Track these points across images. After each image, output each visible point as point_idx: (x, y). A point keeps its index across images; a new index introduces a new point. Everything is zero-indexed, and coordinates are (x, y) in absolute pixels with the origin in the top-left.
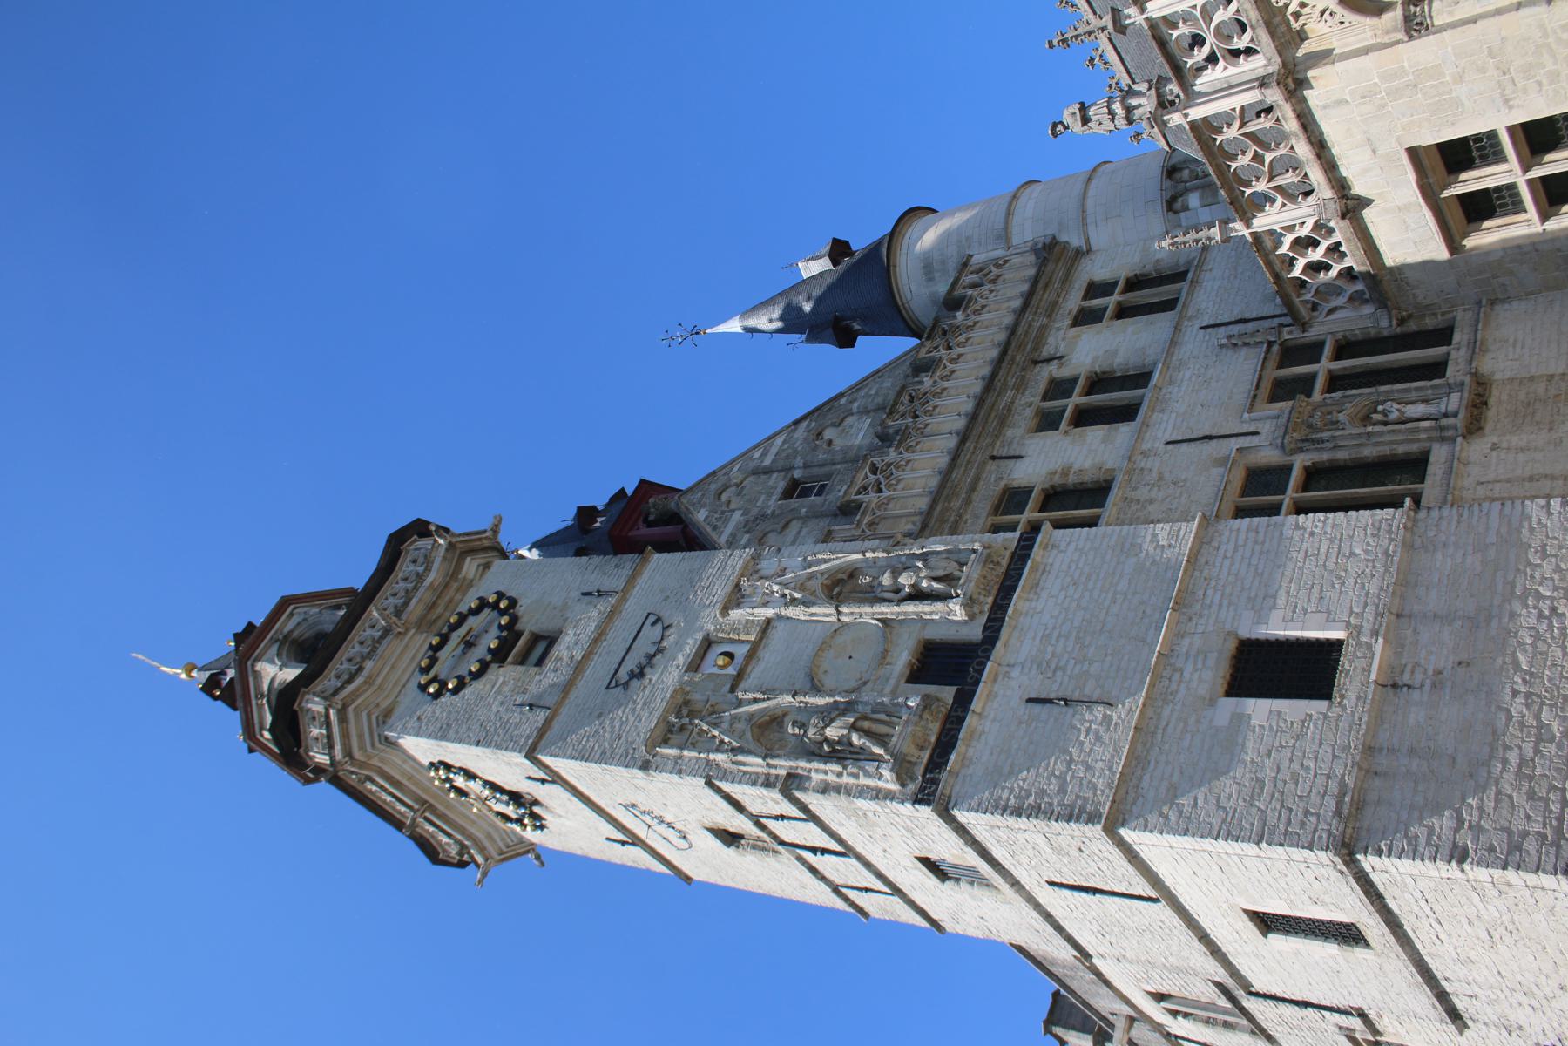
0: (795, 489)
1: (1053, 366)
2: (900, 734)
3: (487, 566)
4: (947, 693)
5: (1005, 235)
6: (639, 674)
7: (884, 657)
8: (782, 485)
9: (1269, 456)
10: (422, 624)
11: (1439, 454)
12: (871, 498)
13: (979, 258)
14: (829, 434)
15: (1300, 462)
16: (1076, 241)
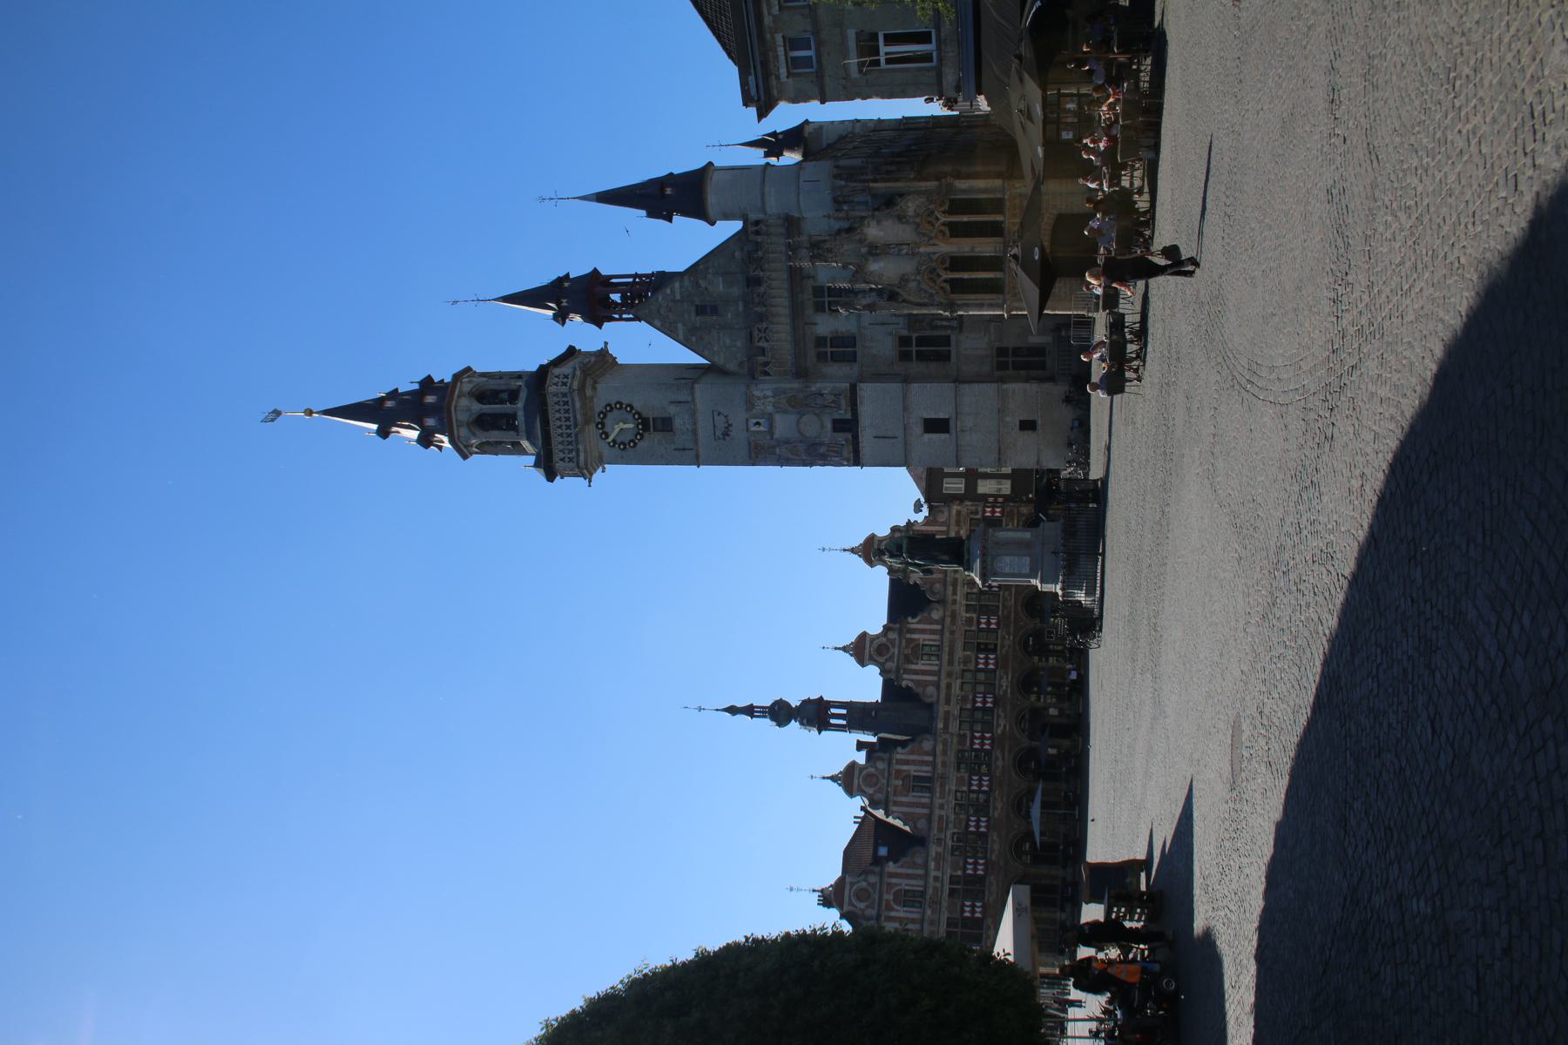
0: (701, 310)
1: (810, 283)
2: (845, 454)
3: (594, 388)
4: (849, 436)
5: (763, 210)
6: (726, 434)
7: (822, 426)
8: (693, 309)
9: (904, 333)
10: (587, 422)
11: (953, 338)
12: (765, 345)
13: (753, 217)
14: (703, 283)
15: (914, 336)
16: (796, 215)
